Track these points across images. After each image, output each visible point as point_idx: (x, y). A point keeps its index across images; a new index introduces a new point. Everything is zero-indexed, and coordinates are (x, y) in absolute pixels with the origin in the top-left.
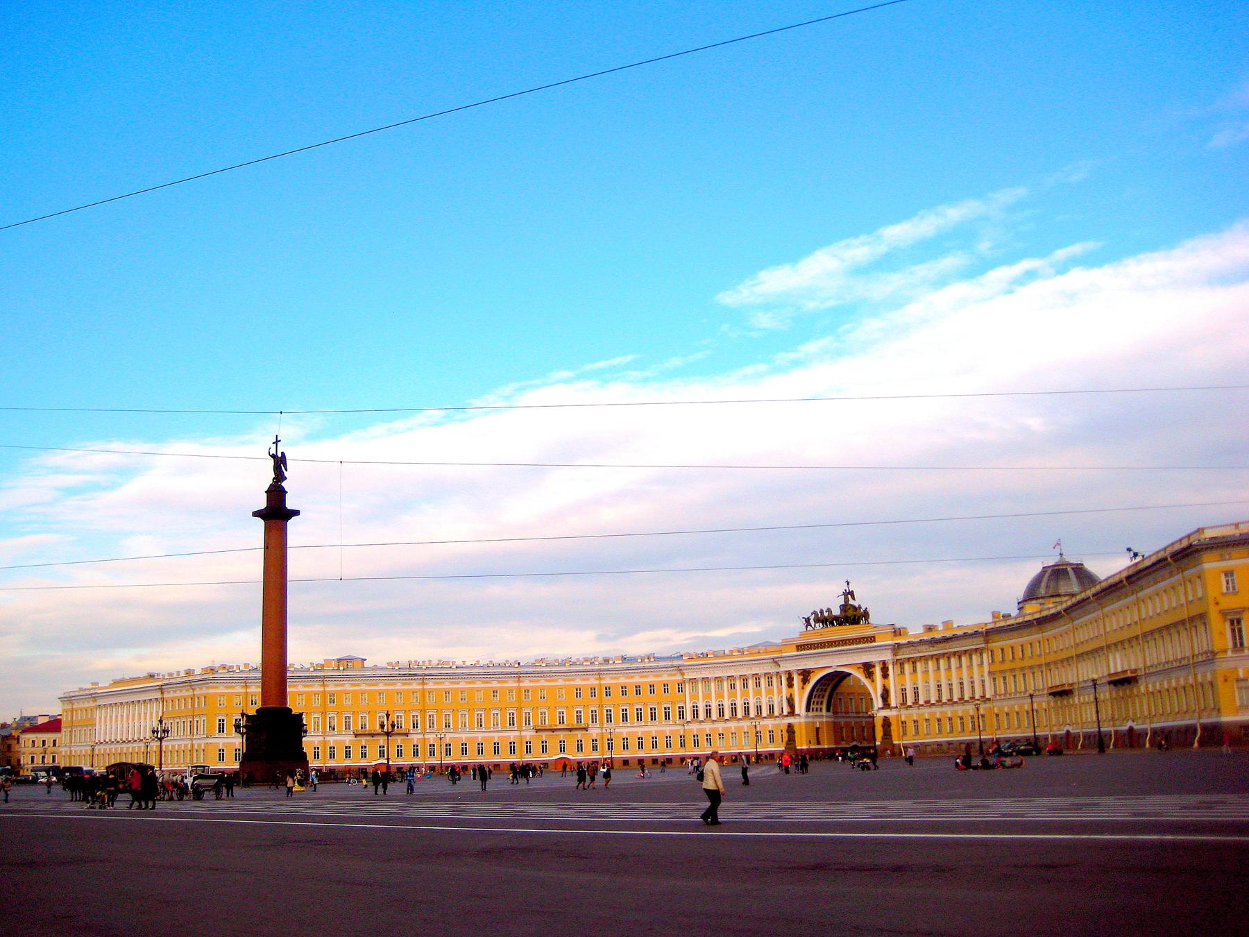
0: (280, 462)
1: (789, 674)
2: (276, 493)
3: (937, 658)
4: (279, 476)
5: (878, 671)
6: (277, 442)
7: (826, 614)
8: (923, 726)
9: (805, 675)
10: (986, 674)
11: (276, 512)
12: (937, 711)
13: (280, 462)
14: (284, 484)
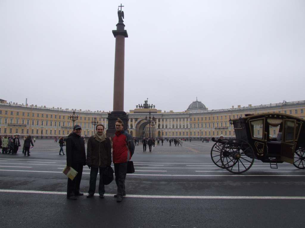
0: (121, 14)
1: (132, 118)
2: (121, 25)
3: (173, 119)
4: (121, 21)
5: (157, 120)
6: (121, 6)
7: (143, 105)
8: (168, 134)
9: (136, 119)
10: (189, 122)
11: (120, 33)
12: (173, 130)
13: (121, 14)
14: (123, 23)
